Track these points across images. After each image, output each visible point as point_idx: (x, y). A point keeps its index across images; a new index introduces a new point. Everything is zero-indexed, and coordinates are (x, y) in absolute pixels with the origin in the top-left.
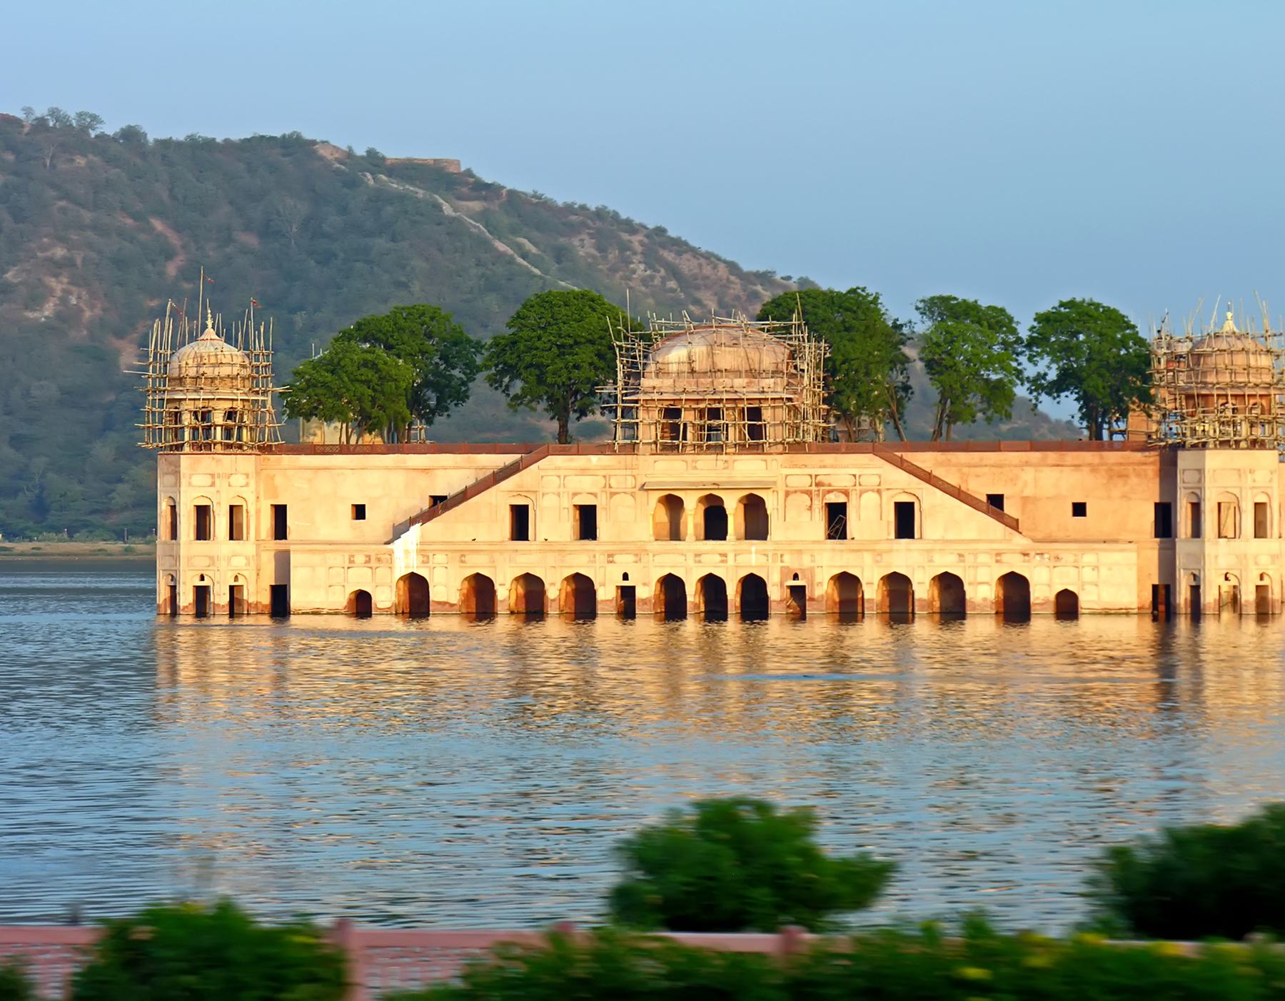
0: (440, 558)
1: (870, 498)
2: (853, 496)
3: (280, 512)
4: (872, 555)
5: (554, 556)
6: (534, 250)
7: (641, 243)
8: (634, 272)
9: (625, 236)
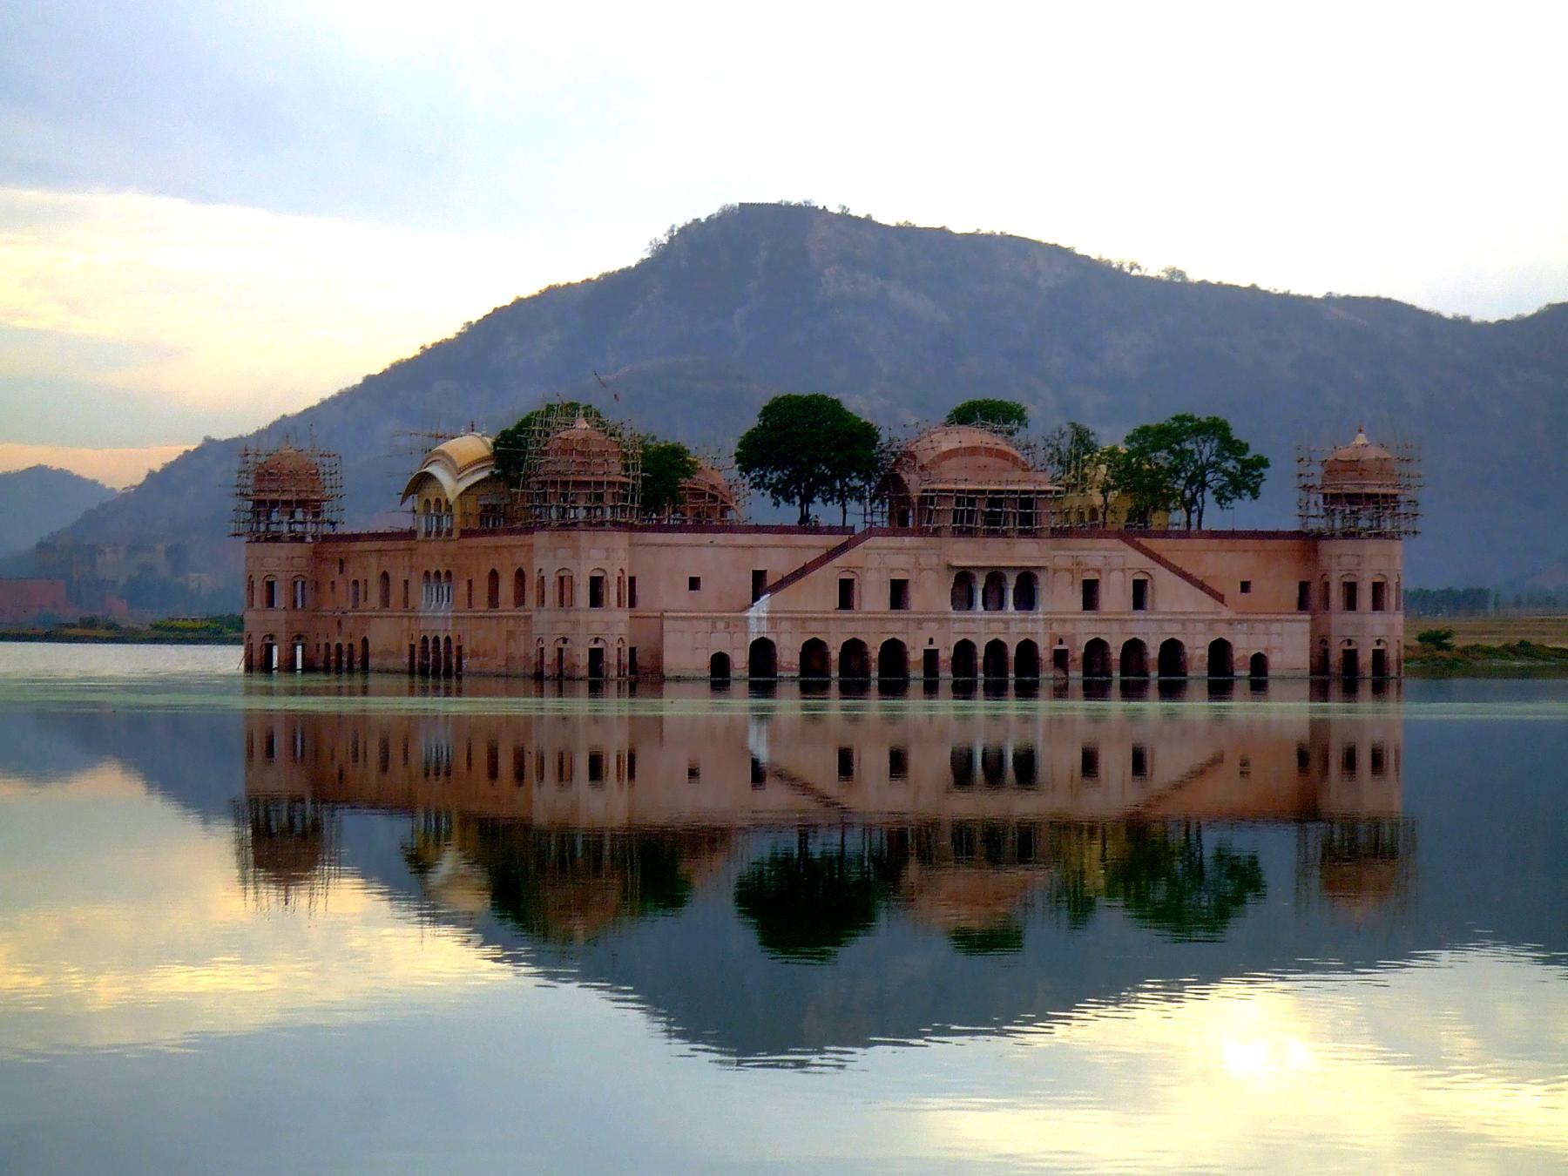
0: (785, 625)
1: (1116, 577)
4: (1116, 625)
5: (872, 624)
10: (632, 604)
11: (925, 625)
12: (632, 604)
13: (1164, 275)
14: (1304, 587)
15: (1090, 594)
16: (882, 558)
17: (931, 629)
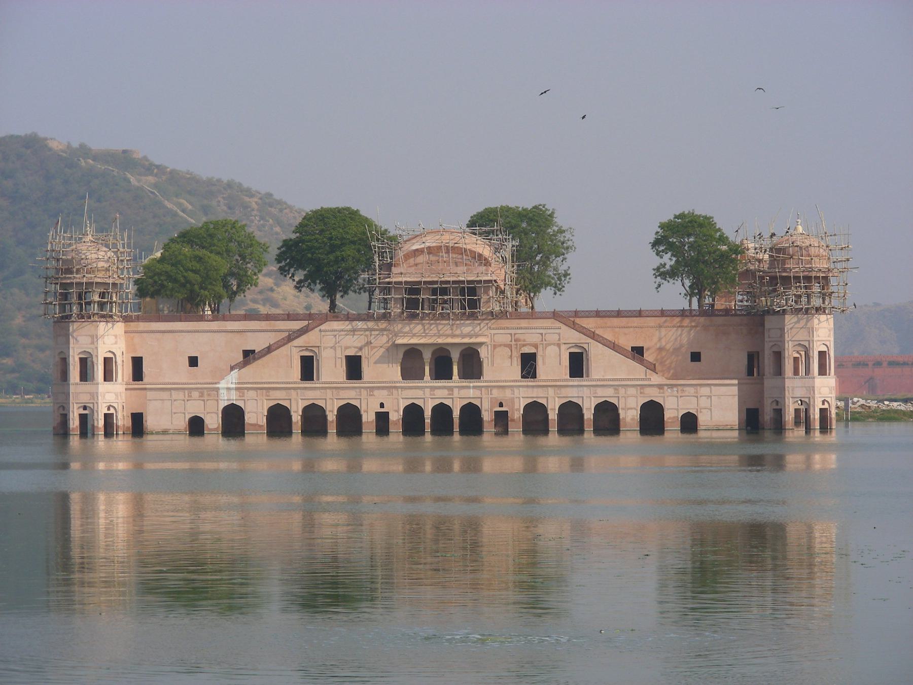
0: (252, 394)
1: (552, 351)
2: (540, 349)
4: (554, 388)
5: (331, 391)
6: (190, 207)
7: (256, 203)
8: (252, 221)
9: (247, 199)
11: (376, 392)
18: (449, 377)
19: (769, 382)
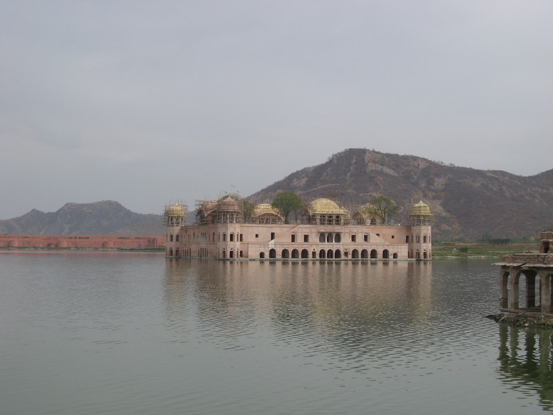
0: (278, 246)
1: (360, 234)
3: (241, 235)
10: (241, 240)
12: (241, 240)
13: (449, 165)
14: (407, 237)
15: (353, 238)
16: (302, 230)
17: (314, 247)
18: (332, 241)
19: (415, 245)
